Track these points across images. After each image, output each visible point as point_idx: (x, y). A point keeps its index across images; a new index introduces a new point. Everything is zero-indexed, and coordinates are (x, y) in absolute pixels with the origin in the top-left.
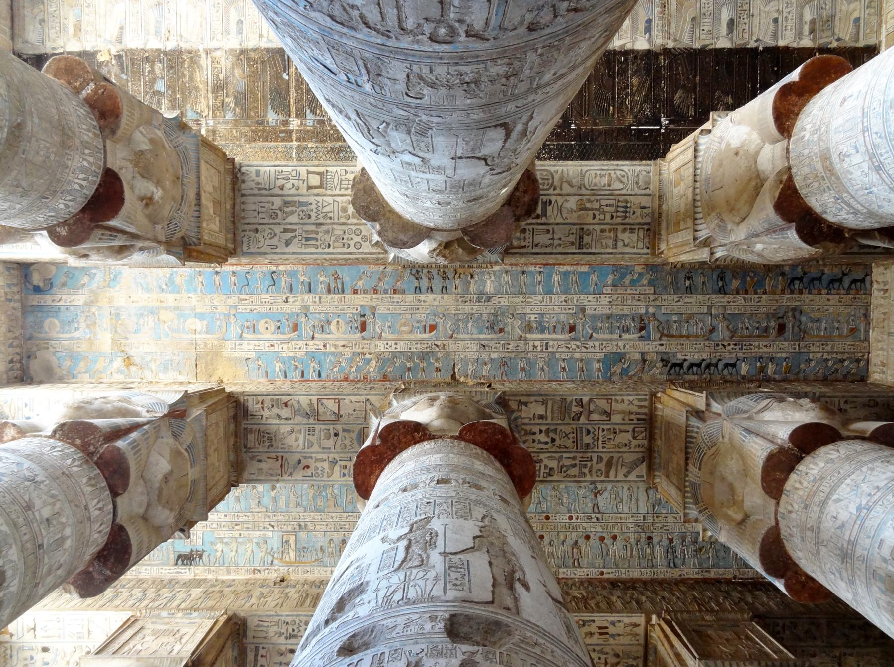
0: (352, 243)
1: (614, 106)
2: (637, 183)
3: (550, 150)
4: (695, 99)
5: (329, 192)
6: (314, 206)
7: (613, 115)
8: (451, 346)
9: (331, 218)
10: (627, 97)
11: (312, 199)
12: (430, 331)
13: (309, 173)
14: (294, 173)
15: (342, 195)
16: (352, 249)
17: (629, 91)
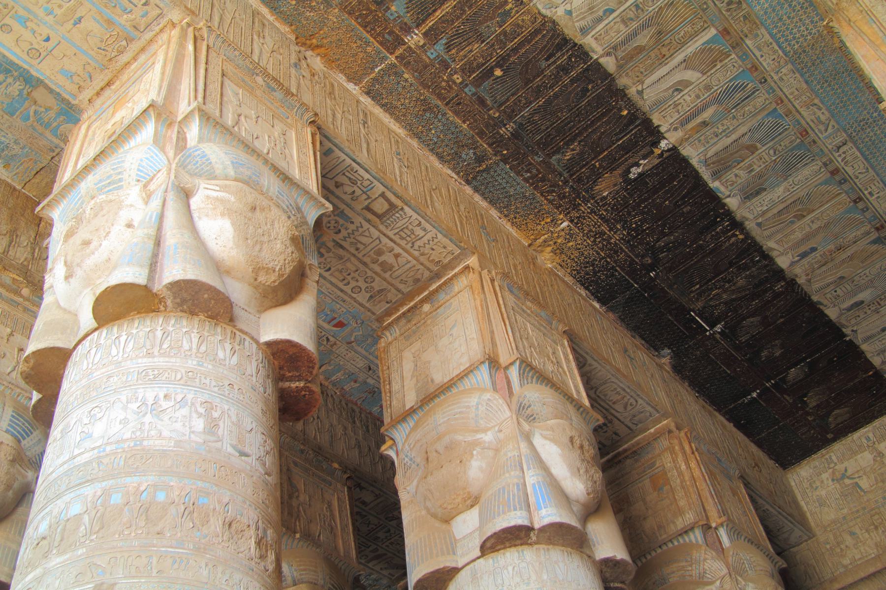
0: (353, 284)
1: (701, 286)
2: (634, 416)
3: (613, 275)
4: (759, 332)
5: (382, 227)
6: (352, 227)
7: (692, 292)
8: (342, 349)
9: (357, 249)
10: (719, 288)
11: (358, 220)
12: (335, 326)
13: (383, 195)
14: (366, 183)
15: (391, 240)
16: (347, 289)
17: (727, 285)
